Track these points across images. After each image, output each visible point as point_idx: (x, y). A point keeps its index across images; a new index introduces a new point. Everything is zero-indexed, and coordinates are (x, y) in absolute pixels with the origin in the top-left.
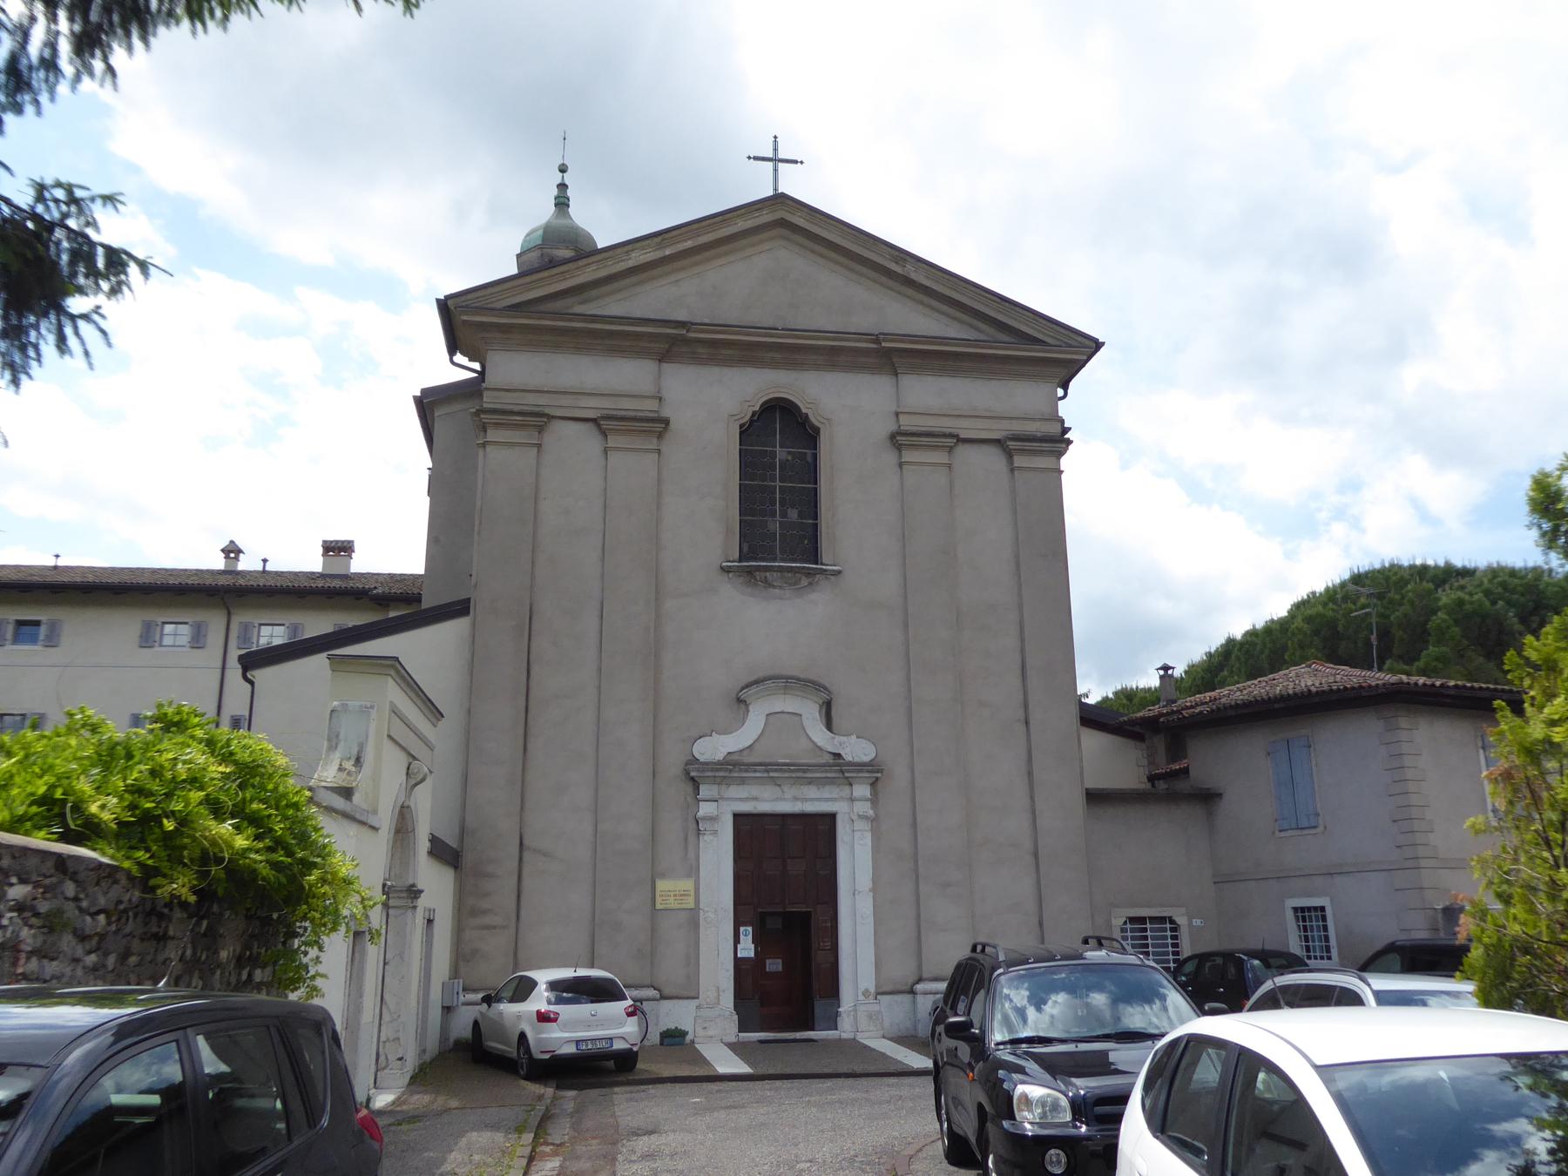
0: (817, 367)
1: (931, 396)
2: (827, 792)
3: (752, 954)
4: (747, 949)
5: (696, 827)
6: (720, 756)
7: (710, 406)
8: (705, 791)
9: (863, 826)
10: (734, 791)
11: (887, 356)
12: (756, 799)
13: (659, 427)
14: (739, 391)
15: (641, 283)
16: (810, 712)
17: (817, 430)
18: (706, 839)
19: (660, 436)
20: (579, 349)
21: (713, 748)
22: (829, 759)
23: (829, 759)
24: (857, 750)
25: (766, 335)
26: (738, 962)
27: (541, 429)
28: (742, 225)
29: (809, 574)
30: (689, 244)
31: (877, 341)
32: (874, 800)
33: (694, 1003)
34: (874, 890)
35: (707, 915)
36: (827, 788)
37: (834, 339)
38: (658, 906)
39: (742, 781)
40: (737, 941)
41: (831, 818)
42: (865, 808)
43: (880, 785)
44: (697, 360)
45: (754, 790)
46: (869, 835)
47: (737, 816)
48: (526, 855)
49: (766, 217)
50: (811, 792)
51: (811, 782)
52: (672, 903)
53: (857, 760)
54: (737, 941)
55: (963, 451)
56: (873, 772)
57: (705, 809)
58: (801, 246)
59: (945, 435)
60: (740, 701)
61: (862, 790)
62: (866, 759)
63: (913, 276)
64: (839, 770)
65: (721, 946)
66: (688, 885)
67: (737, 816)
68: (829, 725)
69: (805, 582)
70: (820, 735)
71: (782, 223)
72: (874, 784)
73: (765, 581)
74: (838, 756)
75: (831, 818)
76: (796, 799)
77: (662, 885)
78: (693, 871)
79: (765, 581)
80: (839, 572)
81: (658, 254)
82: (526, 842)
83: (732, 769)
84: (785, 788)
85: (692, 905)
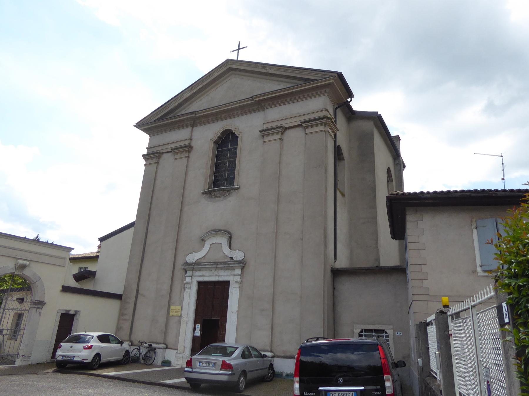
0: (239, 115)
1: (275, 114)
2: (228, 272)
3: (199, 335)
4: (198, 333)
5: (184, 287)
6: (194, 261)
7: (205, 137)
8: (189, 273)
9: (238, 285)
10: (198, 273)
11: (259, 104)
12: (203, 276)
13: (187, 149)
14: (214, 130)
15: (190, 104)
16: (223, 241)
17: (238, 137)
18: (187, 290)
19: (189, 152)
20: (172, 129)
21: (192, 258)
22: (229, 260)
23: (229, 260)
24: (238, 256)
25: (218, 109)
26: (194, 338)
27: (159, 158)
28: (216, 74)
29: (228, 190)
30: (201, 86)
31: (253, 100)
32: (242, 275)
33: (176, 351)
34: (238, 311)
35: (184, 319)
36: (227, 271)
37: (240, 103)
38: (170, 315)
39: (200, 269)
40: (195, 329)
41: (227, 283)
42: (238, 279)
43: (245, 269)
44: (202, 124)
45: (203, 273)
46: (238, 289)
47: (200, 284)
48: (139, 296)
49: (224, 69)
50: (222, 273)
51: (221, 269)
52: (175, 314)
53: (238, 259)
54: (195, 329)
55: (289, 133)
56: (243, 264)
57: (188, 280)
58: (239, 75)
59: (277, 128)
60: (203, 240)
61: (238, 271)
62: (241, 259)
63: (271, 72)
64: (230, 264)
65: (187, 330)
66: (179, 307)
67: (200, 284)
68: (230, 248)
69: (227, 193)
70: (226, 250)
71: (230, 69)
72: (243, 268)
73: (214, 195)
74: (232, 258)
75: (227, 283)
76: (216, 275)
77: (172, 308)
78: (181, 303)
79: (214, 195)
80: (239, 188)
81: (192, 92)
82: (139, 292)
83: (195, 266)
84: (213, 271)
85: (179, 315)
